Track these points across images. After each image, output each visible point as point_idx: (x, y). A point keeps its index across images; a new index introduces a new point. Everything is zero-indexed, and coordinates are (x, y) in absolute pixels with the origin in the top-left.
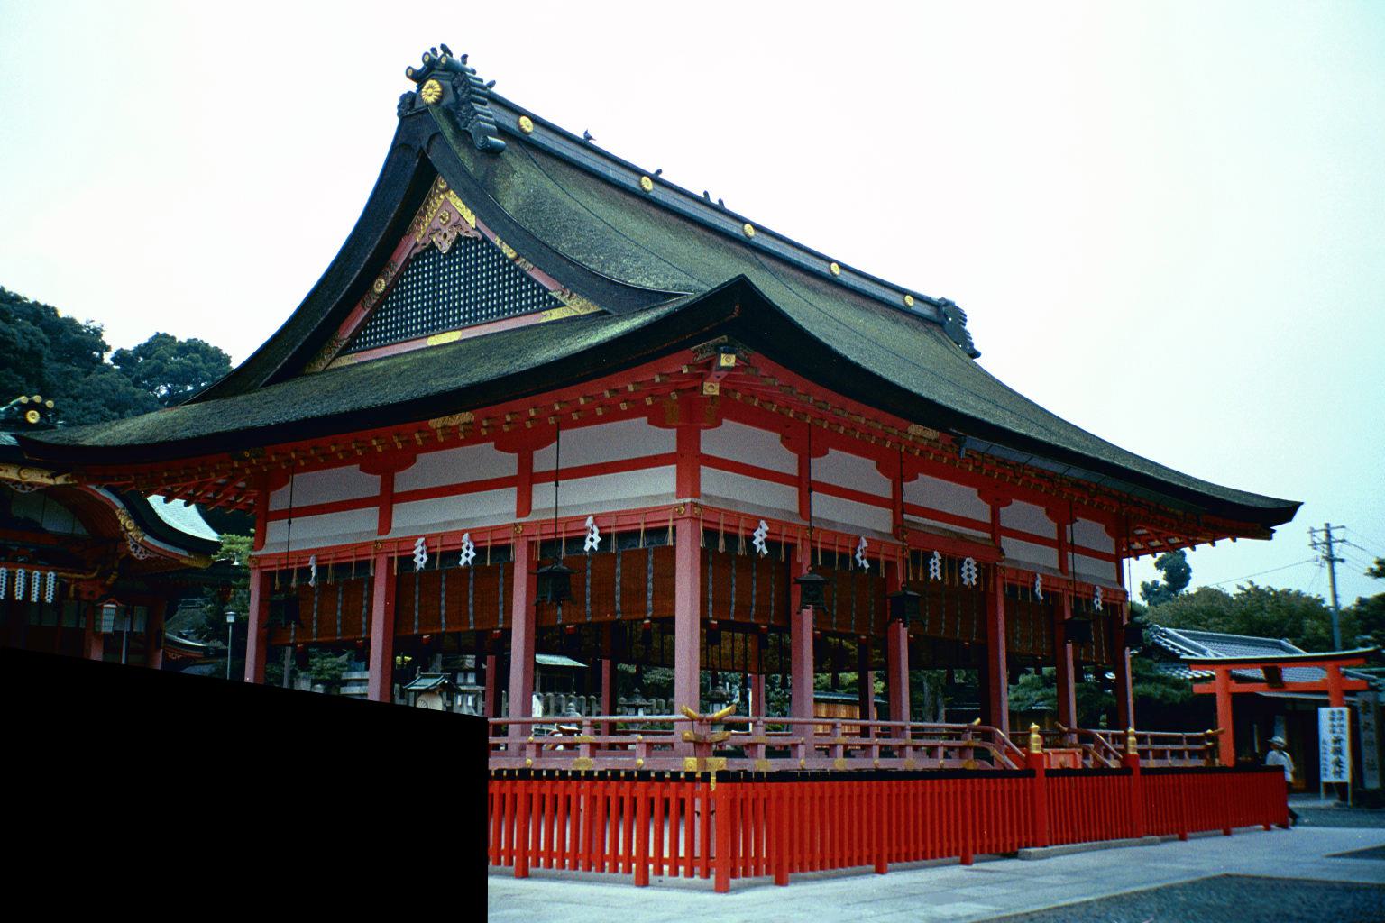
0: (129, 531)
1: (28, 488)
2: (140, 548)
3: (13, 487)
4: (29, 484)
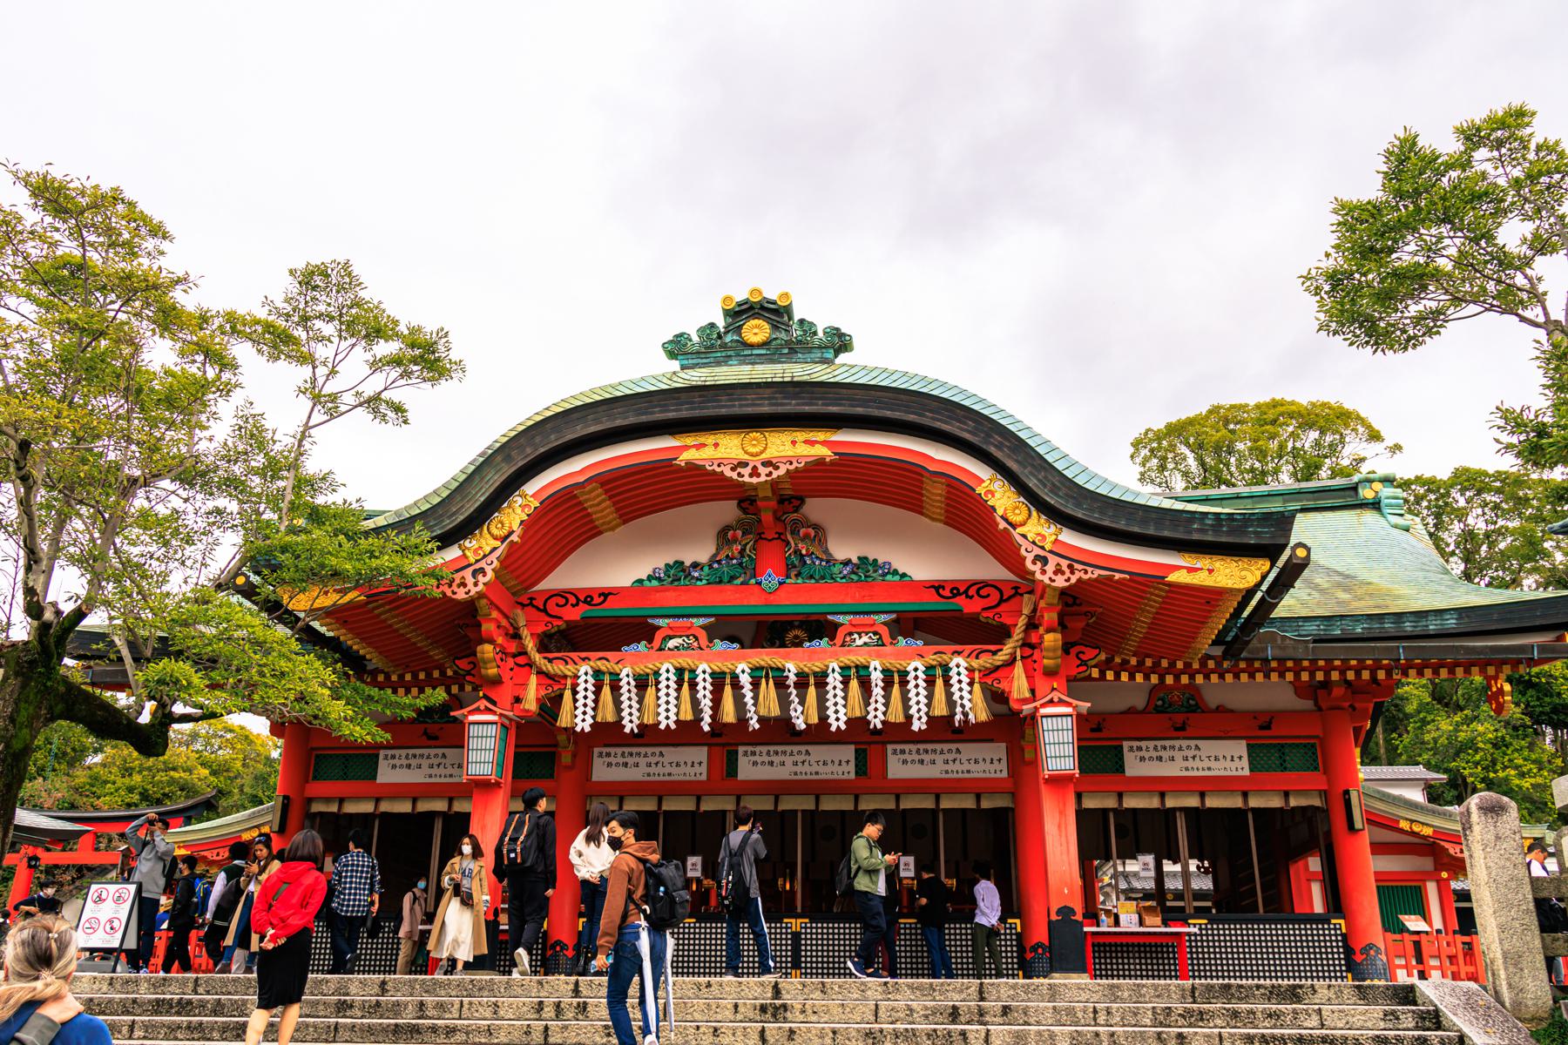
0: (1014, 526)
1: (763, 471)
2: (1053, 561)
3: (734, 475)
4: (767, 463)
